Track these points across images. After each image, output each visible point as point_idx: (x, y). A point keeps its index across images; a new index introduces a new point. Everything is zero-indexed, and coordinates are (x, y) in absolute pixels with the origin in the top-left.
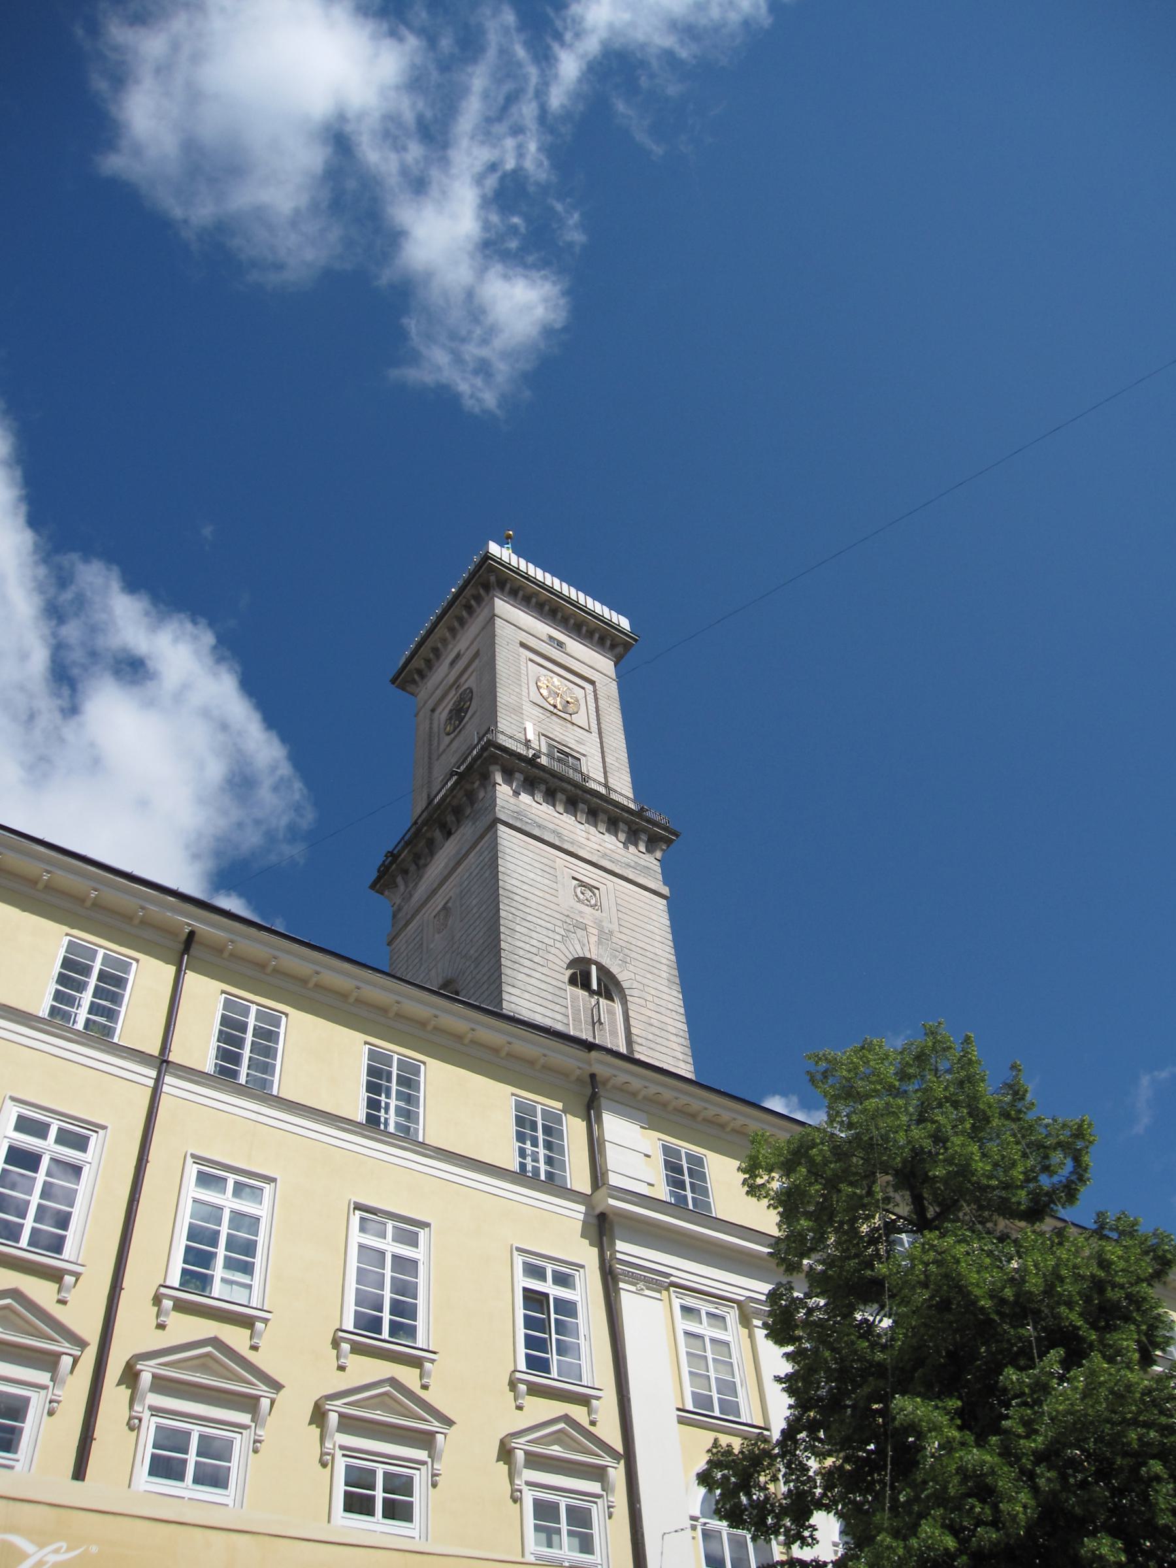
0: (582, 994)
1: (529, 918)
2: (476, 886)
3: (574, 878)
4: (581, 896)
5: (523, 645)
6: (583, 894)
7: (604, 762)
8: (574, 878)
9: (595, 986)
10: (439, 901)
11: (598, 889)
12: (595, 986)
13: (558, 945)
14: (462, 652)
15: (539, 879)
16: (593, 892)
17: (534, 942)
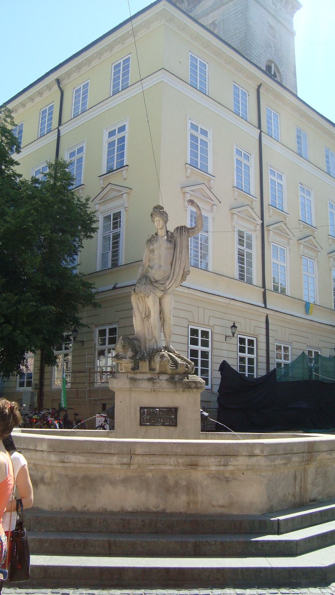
3: (268, 23)
4: (270, 31)
9: (273, 73)
12: (273, 73)
13: (264, 53)
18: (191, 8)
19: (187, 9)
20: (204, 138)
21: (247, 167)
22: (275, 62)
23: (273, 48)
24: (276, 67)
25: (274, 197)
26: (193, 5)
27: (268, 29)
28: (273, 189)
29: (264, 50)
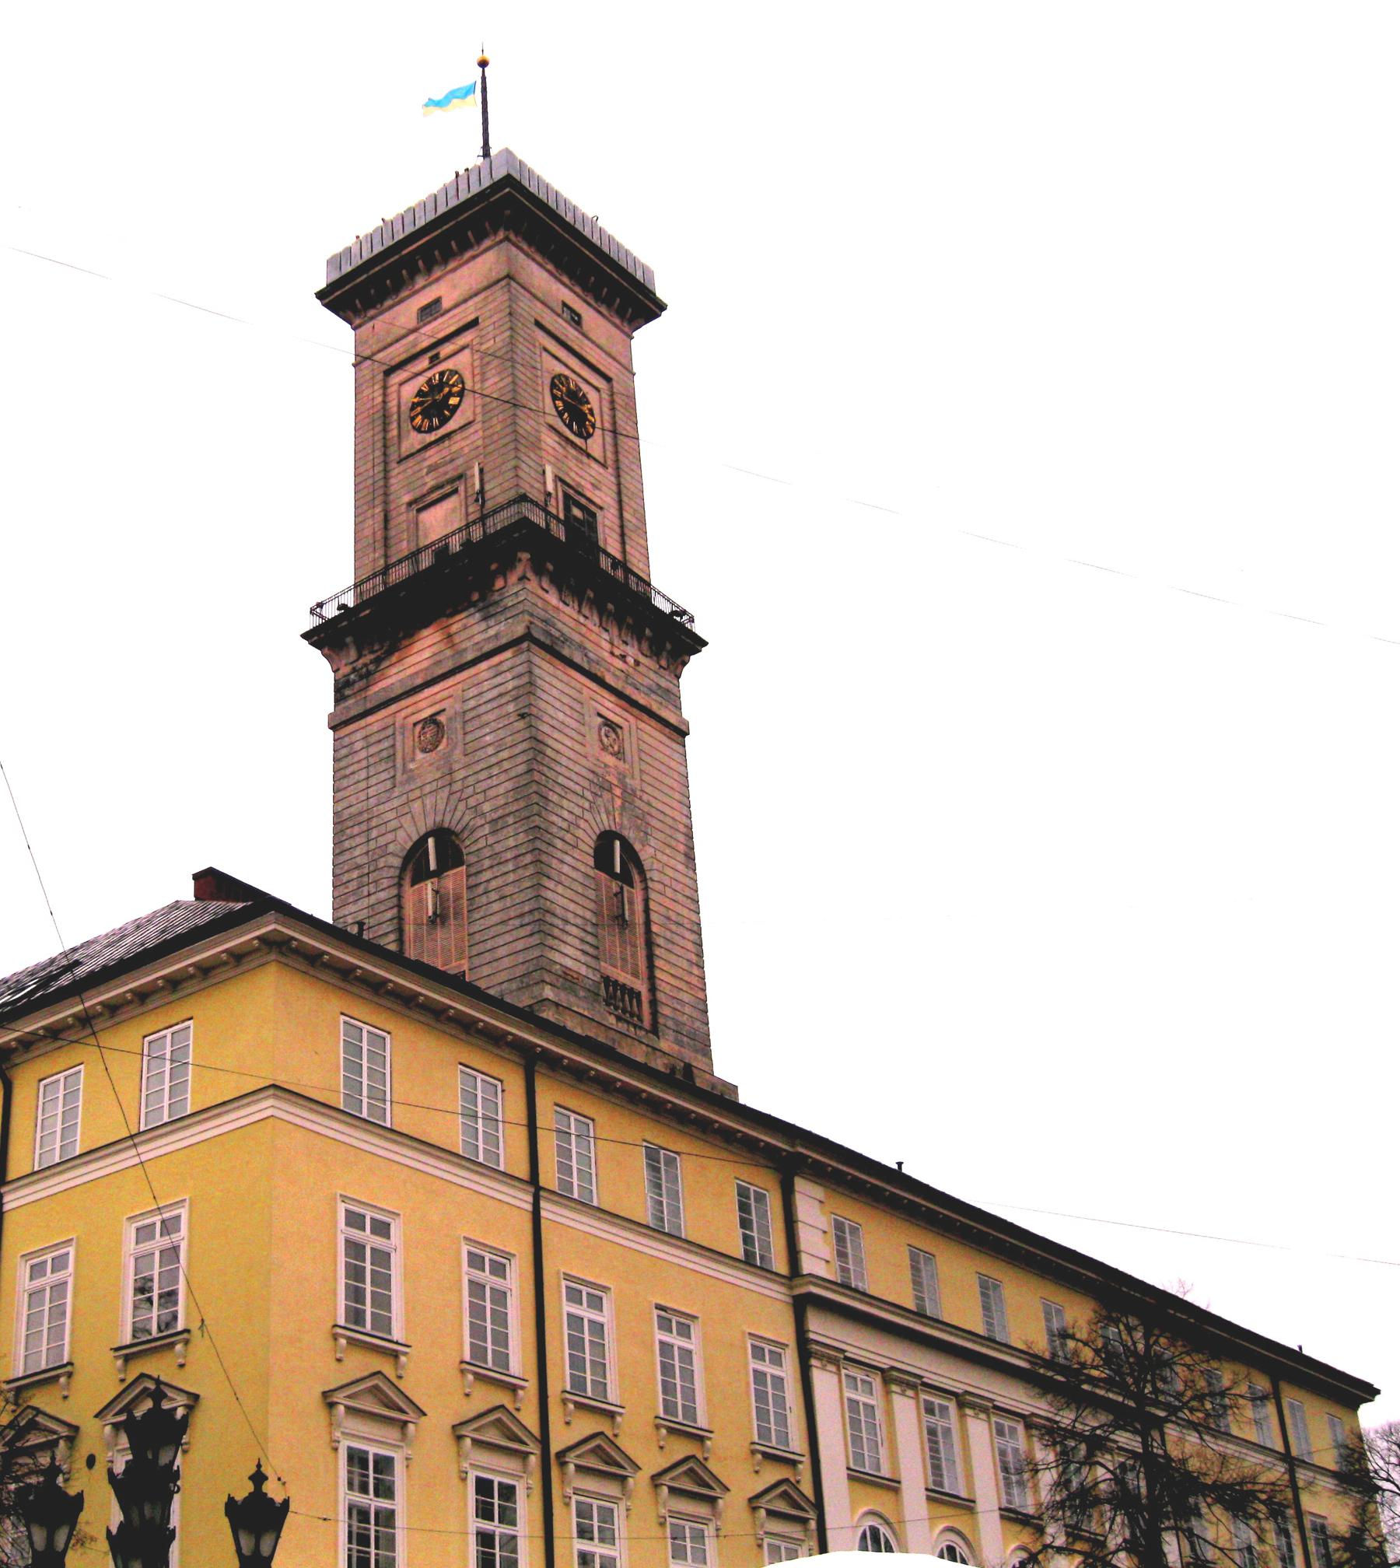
0: (603, 876)
1: (561, 780)
2: (491, 717)
3: (600, 715)
4: (605, 740)
5: (538, 324)
6: (607, 736)
7: (621, 517)
8: (600, 715)
9: (618, 870)
10: (424, 705)
11: (621, 728)
12: (618, 870)
13: (587, 815)
14: (446, 304)
15: (568, 721)
16: (616, 734)
17: (565, 814)
18: (366, 665)
19: (355, 665)
20: (378, 1242)
21: (500, 1297)
22: (625, 833)
23: (618, 792)
24: (627, 847)
25: (577, 1363)
26: (372, 657)
27: (600, 735)
28: (576, 1343)
29: (587, 805)
